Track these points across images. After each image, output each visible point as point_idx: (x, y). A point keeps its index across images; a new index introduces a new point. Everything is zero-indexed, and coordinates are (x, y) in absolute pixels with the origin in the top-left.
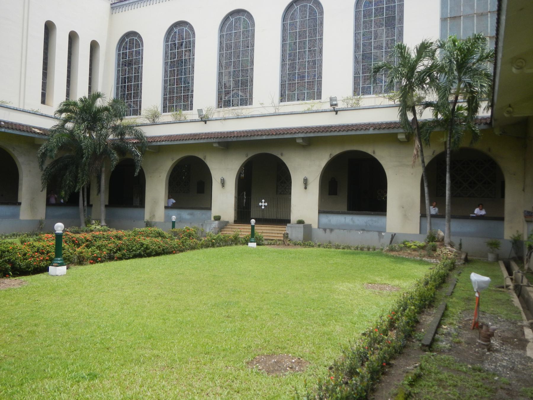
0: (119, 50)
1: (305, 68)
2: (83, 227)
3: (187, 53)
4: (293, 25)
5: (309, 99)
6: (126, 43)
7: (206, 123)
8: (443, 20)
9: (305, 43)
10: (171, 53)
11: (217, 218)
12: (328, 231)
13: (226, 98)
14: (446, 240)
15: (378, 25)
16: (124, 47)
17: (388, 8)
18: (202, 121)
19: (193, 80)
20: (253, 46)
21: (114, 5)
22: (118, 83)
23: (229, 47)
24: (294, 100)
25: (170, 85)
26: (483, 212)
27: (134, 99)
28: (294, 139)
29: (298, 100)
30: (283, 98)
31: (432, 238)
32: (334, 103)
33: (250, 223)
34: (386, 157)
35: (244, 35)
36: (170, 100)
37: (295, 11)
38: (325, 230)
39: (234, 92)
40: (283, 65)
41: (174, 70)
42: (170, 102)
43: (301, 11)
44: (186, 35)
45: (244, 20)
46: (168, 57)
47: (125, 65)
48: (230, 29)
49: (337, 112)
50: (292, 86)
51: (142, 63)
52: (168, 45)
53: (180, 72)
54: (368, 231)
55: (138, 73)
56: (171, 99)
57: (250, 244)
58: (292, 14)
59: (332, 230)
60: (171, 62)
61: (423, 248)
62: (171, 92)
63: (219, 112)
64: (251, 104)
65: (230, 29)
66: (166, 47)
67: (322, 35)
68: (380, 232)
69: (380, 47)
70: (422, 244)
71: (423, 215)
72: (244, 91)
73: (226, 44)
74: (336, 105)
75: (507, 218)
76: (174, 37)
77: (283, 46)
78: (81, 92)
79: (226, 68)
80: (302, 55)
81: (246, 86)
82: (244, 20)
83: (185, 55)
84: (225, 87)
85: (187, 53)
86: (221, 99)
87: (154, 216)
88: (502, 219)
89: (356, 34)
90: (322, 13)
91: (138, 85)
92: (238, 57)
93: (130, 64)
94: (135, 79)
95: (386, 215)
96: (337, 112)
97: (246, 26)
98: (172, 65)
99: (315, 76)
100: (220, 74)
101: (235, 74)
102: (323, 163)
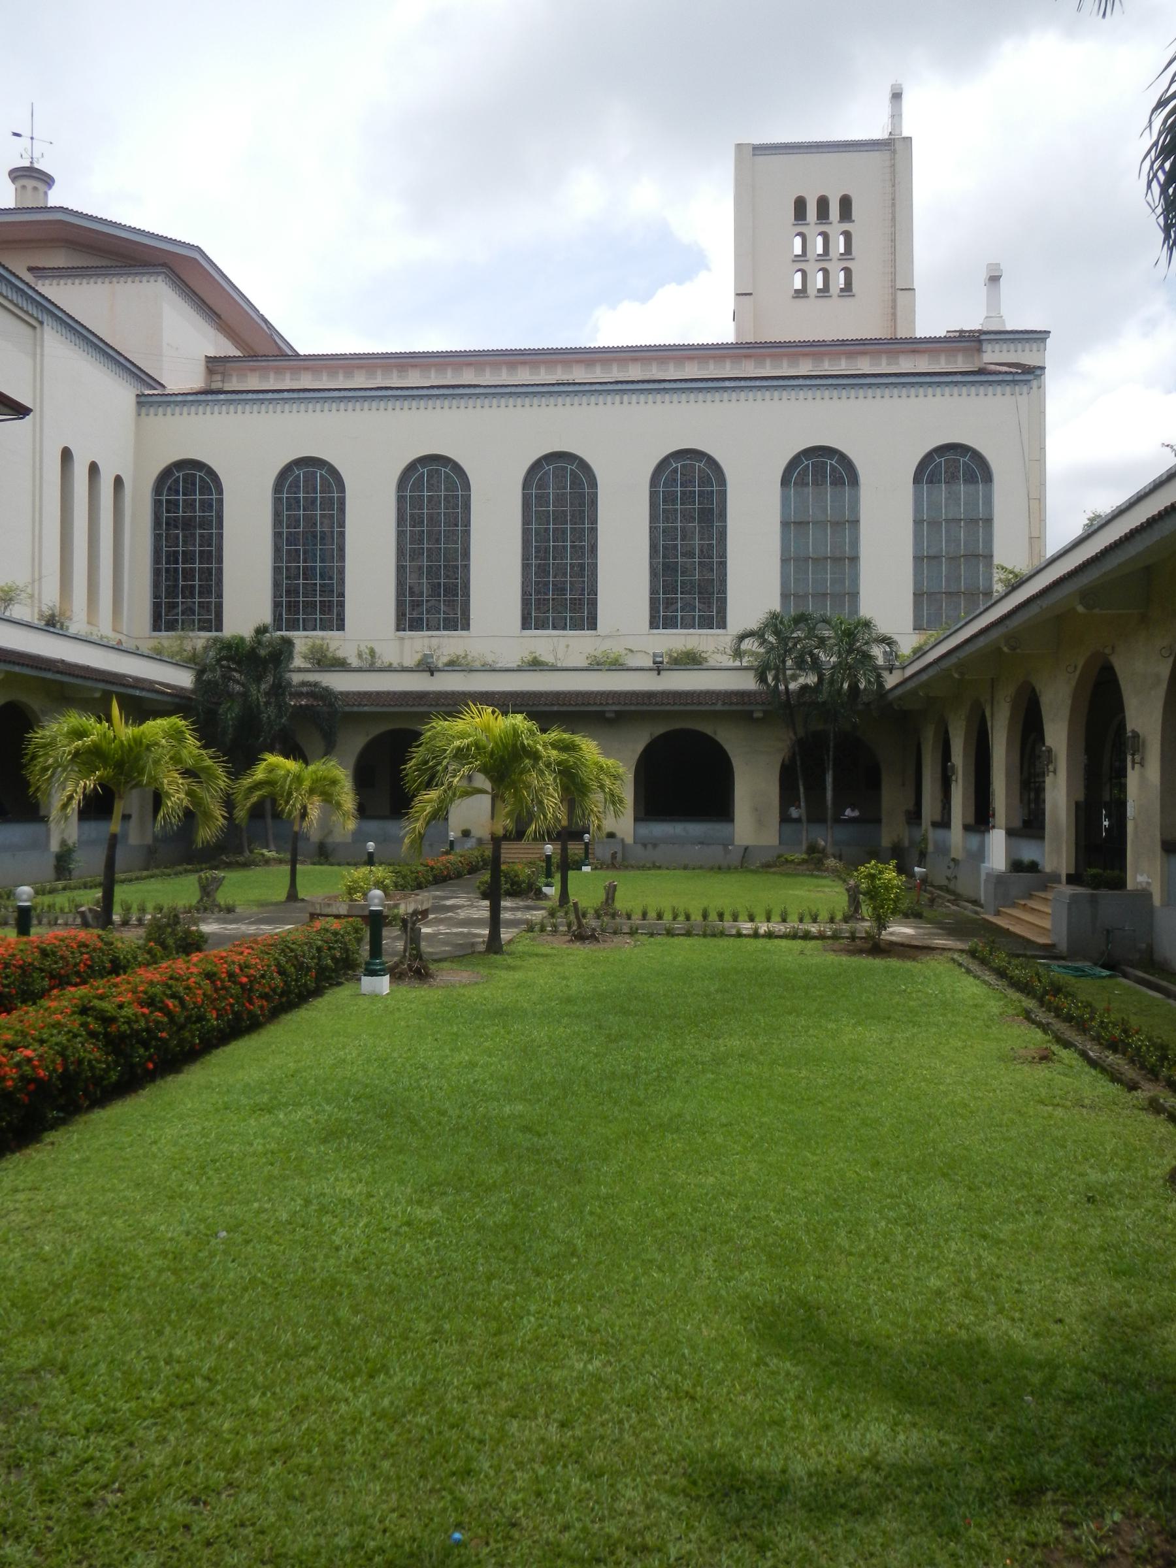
1: (565, 575)
2: (247, 854)
3: (326, 521)
4: (542, 499)
5: (574, 627)
6: (177, 481)
8: (785, 524)
9: (564, 531)
10: (289, 516)
11: (466, 834)
12: (650, 847)
14: (829, 850)
15: (687, 517)
16: (170, 489)
17: (701, 493)
19: (342, 571)
20: (467, 524)
21: (143, 399)
22: (157, 559)
23: (417, 521)
24: (548, 628)
26: (856, 813)
28: (604, 712)
29: (554, 628)
30: (526, 624)
31: (812, 849)
32: (659, 659)
33: (582, 840)
34: (732, 741)
35: (449, 502)
37: (545, 473)
38: (645, 845)
39: (430, 604)
40: (526, 567)
42: (289, 611)
43: (555, 476)
45: (447, 476)
47: (176, 527)
48: (418, 486)
49: (659, 671)
50: (541, 604)
51: (220, 525)
53: (309, 555)
54: (709, 844)
55: (210, 545)
56: (292, 607)
57: (586, 869)
58: (540, 479)
59: (655, 846)
60: (289, 534)
61: (804, 861)
63: (403, 639)
64: (466, 627)
65: (418, 486)
66: (277, 501)
67: (594, 521)
68: (725, 846)
69: (689, 554)
70: (804, 856)
71: (785, 819)
72: (451, 604)
73: (412, 515)
74: (661, 663)
75: (884, 820)
76: (295, 485)
77: (526, 532)
79: (412, 560)
80: (560, 553)
81: (454, 596)
82: (447, 476)
83: (321, 523)
84: (412, 594)
85: (326, 521)
86: (404, 615)
87: (330, 832)
88: (878, 821)
89: (653, 530)
90: (593, 483)
91: (210, 570)
92: (438, 541)
93: (188, 524)
94: (201, 557)
95: (732, 820)
96: (659, 671)
97: (451, 487)
98: (292, 539)
99: (583, 589)
100: (400, 569)
101: (433, 572)
102: (640, 748)
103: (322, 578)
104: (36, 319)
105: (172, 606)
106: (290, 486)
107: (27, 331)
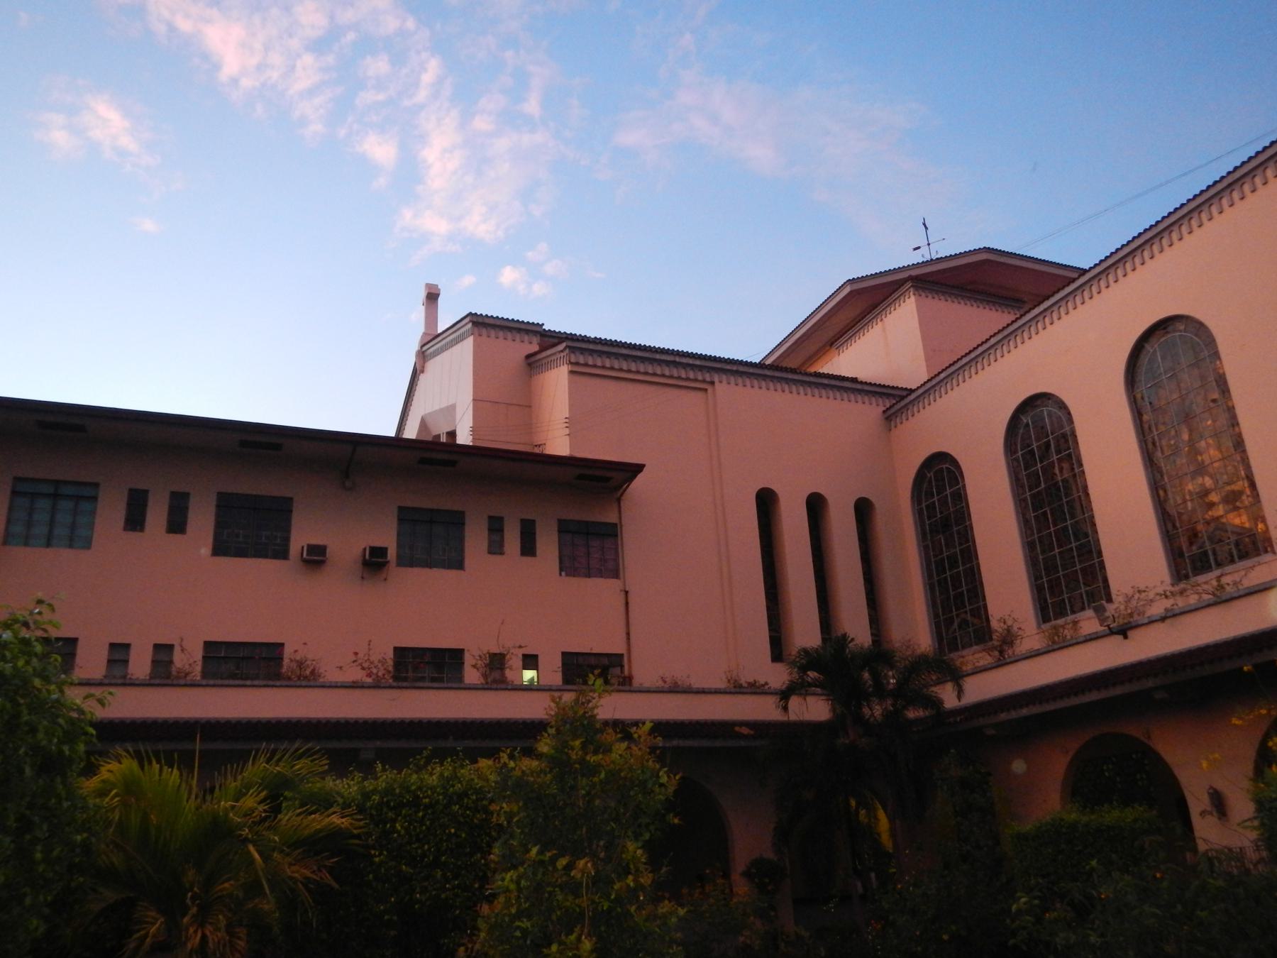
0: (920, 503)
6: (930, 482)
7: (1126, 637)
10: (1028, 476)
13: (1194, 548)
18: (1112, 632)
22: (930, 576)
25: (1043, 552)
27: (970, 604)
36: (1051, 588)
41: (1045, 513)
42: (1052, 594)
44: (1052, 424)
46: (1023, 487)
52: (1017, 460)
55: (967, 541)
60: (1033, 496)
62: (1051, 568)
78: (805, 632)
83: (1061, 470)
85: (1066, 465)
86: (1181, 554)
91: (972, 569)
98: (1038, 502)
103: (1077, 539)
104: (704, 381)
105: (950, 622)
106: (1023, 439)
107: (700, 394)
